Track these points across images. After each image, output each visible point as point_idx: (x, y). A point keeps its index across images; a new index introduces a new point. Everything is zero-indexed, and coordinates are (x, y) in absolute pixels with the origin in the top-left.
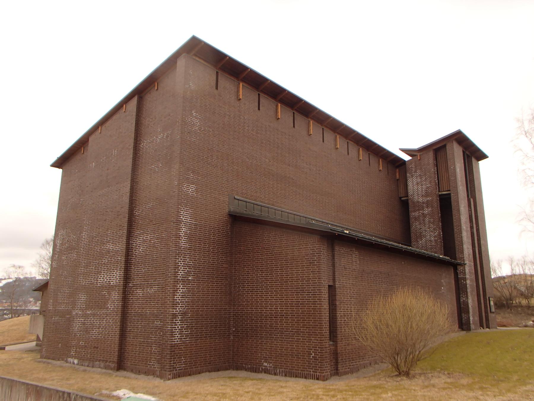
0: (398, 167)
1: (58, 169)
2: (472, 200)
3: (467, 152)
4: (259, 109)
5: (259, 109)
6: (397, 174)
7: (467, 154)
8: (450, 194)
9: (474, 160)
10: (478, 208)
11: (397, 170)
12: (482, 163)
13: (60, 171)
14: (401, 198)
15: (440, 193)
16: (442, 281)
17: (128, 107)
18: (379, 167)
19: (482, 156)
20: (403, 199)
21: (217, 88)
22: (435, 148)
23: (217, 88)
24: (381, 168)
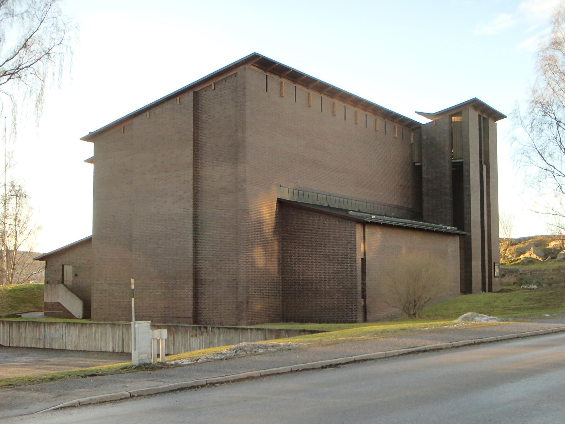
0: (414, 130)
1: (86, 142)
2: (484, 167)
3: (484, 116)
4: (296, 101)
5: (296, 101)
6: (412, 139)
7: (484, 118)
8: (462, 163)
9: (490, 121)
10: (491, 174)
11: (412, 134)
12: (499, 123)
13: (91, 145)
14: (414, 163)
15: (454, 161)
16: (448, 250)
17: (182, 100)
18: (394, 135)
19: (500, 116)
20: (416, 164)
21: (267, 91)
22: (451, 113)
23: (267, 91)
24: (396, 136)
